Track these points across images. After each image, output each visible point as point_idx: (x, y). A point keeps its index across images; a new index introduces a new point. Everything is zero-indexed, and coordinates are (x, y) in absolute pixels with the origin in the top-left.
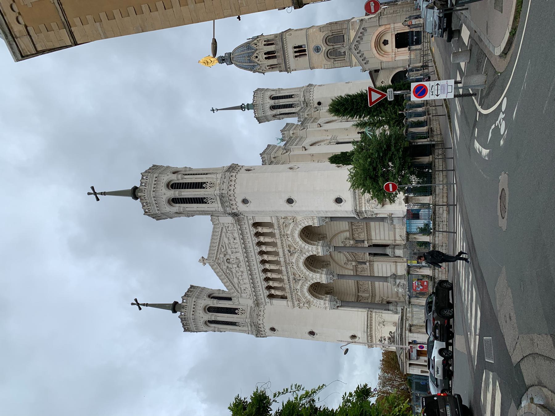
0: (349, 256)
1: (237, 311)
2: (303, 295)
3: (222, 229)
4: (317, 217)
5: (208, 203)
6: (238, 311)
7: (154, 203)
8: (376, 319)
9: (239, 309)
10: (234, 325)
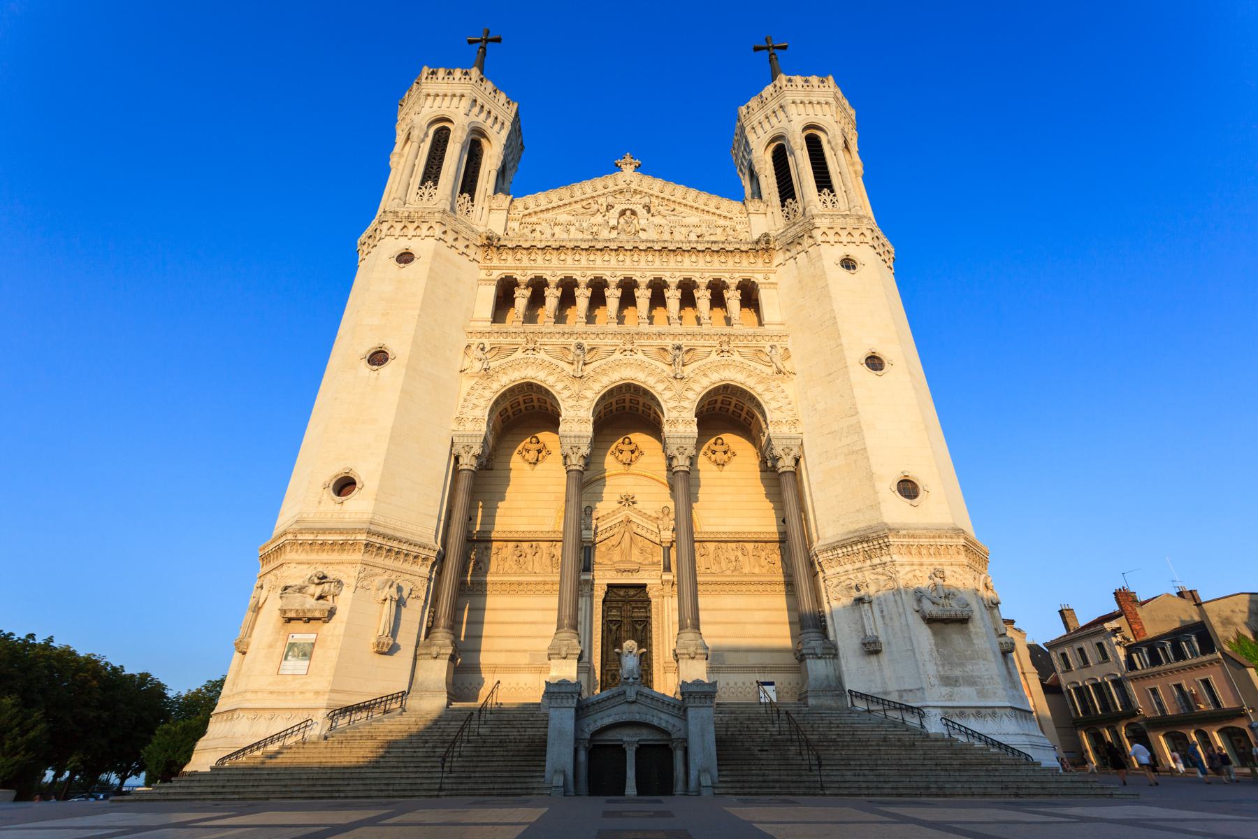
1: (466, 195)
2: (513, 366)
4: (802, 433)
8: (407, 577)
9: (473, 206)
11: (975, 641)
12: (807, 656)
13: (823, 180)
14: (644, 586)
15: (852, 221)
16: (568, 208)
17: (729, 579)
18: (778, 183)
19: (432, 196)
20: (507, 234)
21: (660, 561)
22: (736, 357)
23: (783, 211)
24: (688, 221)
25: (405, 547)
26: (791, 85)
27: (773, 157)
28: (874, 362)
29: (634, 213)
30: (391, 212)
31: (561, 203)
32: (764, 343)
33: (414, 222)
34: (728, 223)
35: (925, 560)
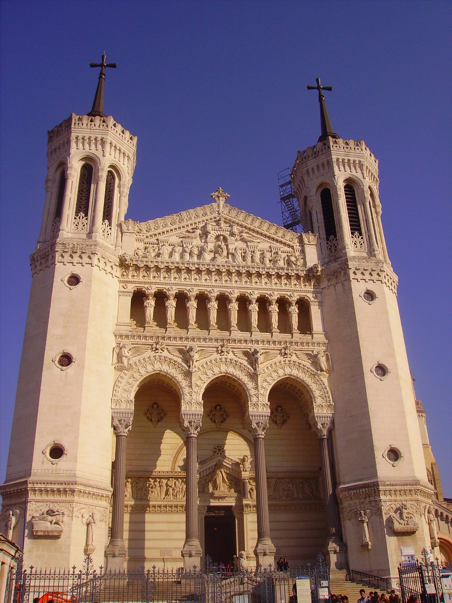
0: (208, 467)
3: (289, 246)
5: (352, 237)
6: (108, 226)
7: (349, 158)
8: (97, 508)
9: (110, 229)
10: (77, 208)
11: (418, 543)
12: (330, 552)
13: (355, 227)
14: (231, 506)
15: (372, 264)
16: (178, 231)
17: (284, 502)
18: (324, 218)
19: (84, 226)
20: (136, 254)
21: (240, 490)
22: (294, 358)
23: (327, 243)
24: (261, 246)
25: (95, 490)
26: (336, 147)
27: (321, 196)
28: (382, 370)
29: (225, 239)
30: (61, 244)
31: (173, 227)
32: (314, 348)
33: (77, 252)
34: (290, 249)
35: (398, 498)
